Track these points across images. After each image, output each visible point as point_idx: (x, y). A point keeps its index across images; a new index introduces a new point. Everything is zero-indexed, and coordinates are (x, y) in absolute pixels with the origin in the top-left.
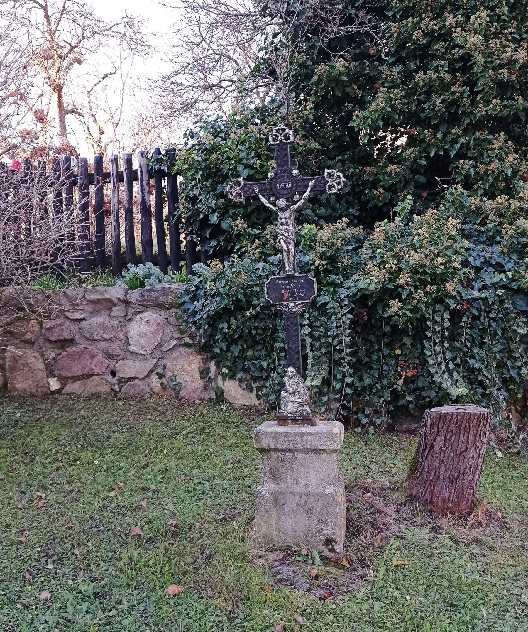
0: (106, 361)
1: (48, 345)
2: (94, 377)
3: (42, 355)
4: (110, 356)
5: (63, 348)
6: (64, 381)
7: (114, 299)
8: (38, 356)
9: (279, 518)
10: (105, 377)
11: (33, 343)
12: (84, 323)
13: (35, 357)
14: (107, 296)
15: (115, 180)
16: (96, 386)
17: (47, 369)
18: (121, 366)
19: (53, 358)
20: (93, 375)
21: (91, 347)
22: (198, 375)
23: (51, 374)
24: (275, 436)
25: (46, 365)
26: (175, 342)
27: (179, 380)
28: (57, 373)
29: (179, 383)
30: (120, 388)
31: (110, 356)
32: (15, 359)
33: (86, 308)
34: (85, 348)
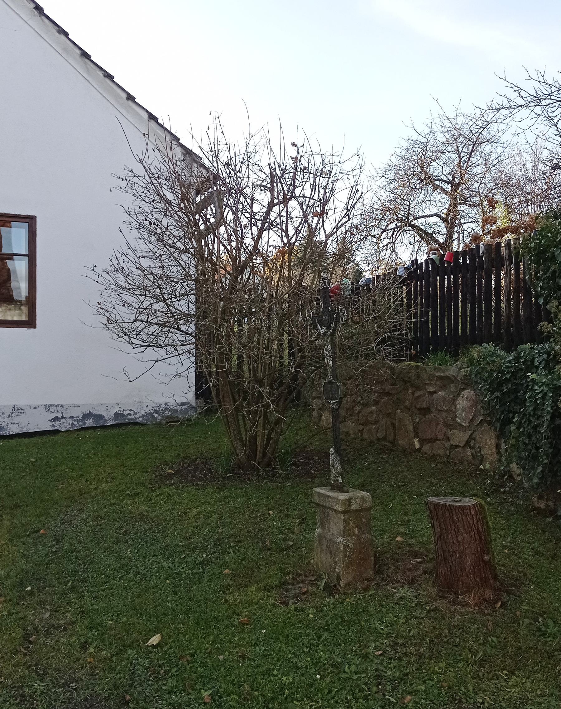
0: (445, 429)
1: (416, 411)
2: (438, 442)
3: (412, 420)
4: (447, 426)
5: (424, 415)
6: (421, 442)
7: (451, 376)
8: (411, 420)
9: (321, 554)
10: (444, 442)
11: (409, 409)
12: (435, 395)
13: (409, 420)
14: (447, 374)
15: (508, 263)
16: (438, 449)
17: (414, 431)
18: (451, 434)
19: (418, 423)
20: (437, 439)
21: (438, 416)
22: (494, 450)
23: (417, 436)
24: (319, 494)
25: (414, 428)
26: (481, 418)
27: (482, 453)
28: (420, 435)
29: (482, 455)
30: (450, 453)
31: (447, 426)
32: (400, 420)
33: (438, 383)
34: (435, 416)
